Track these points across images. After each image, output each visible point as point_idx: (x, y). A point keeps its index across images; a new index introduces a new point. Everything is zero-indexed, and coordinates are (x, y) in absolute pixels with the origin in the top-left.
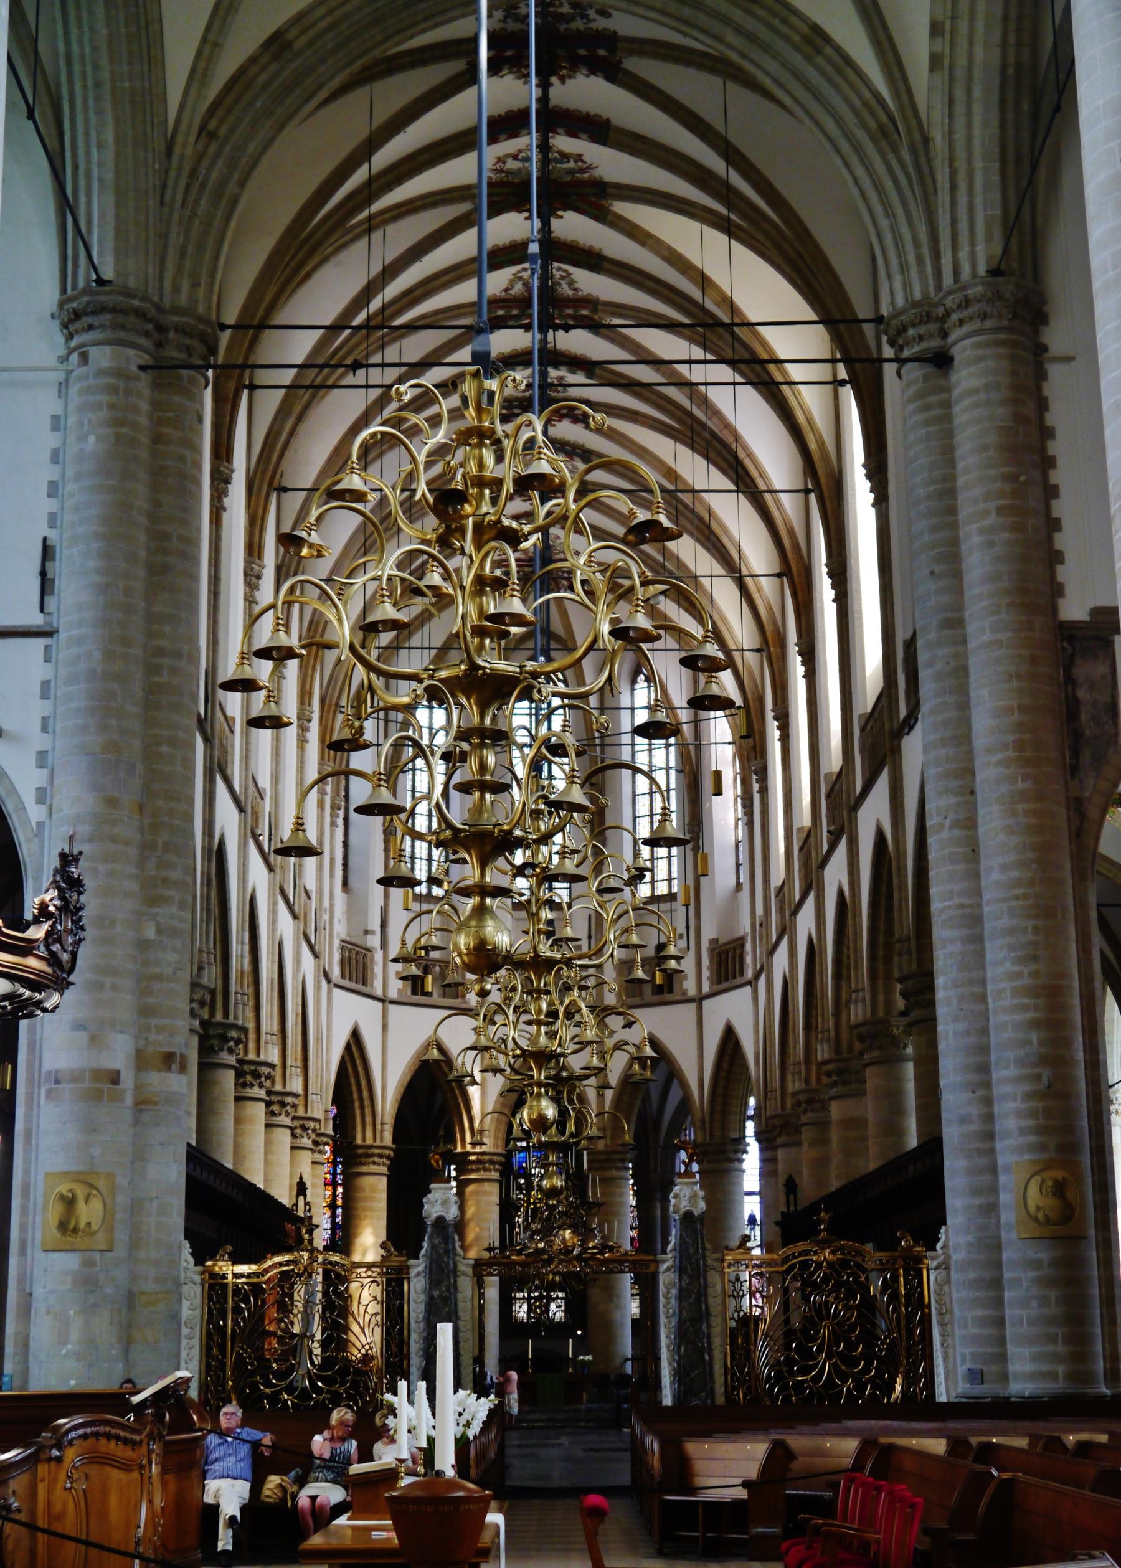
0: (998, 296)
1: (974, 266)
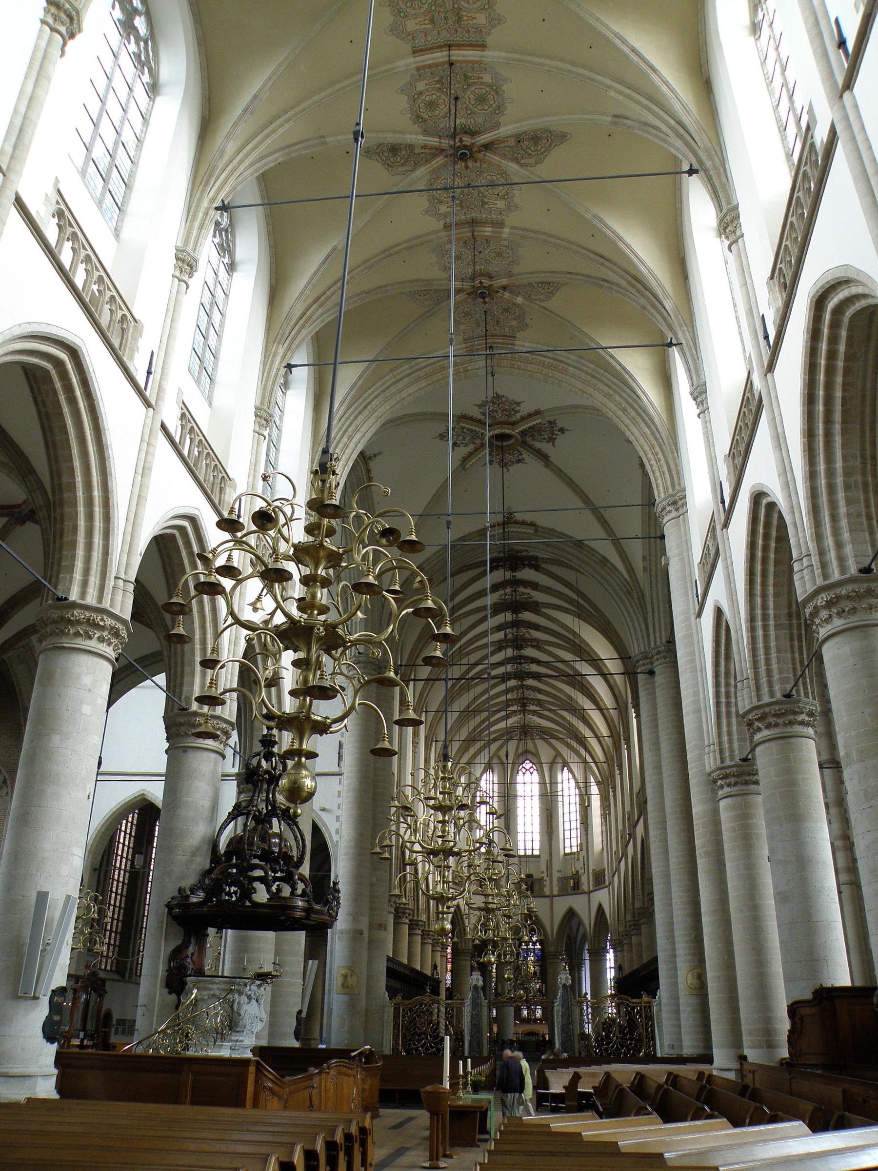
1: (661, 639)
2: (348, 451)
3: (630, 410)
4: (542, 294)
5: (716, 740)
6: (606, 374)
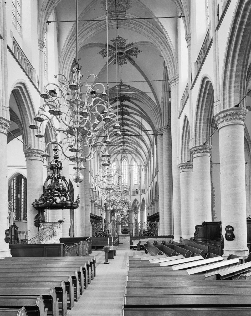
0: (168, 128)
2: (70, 58)
5: (181, 156)
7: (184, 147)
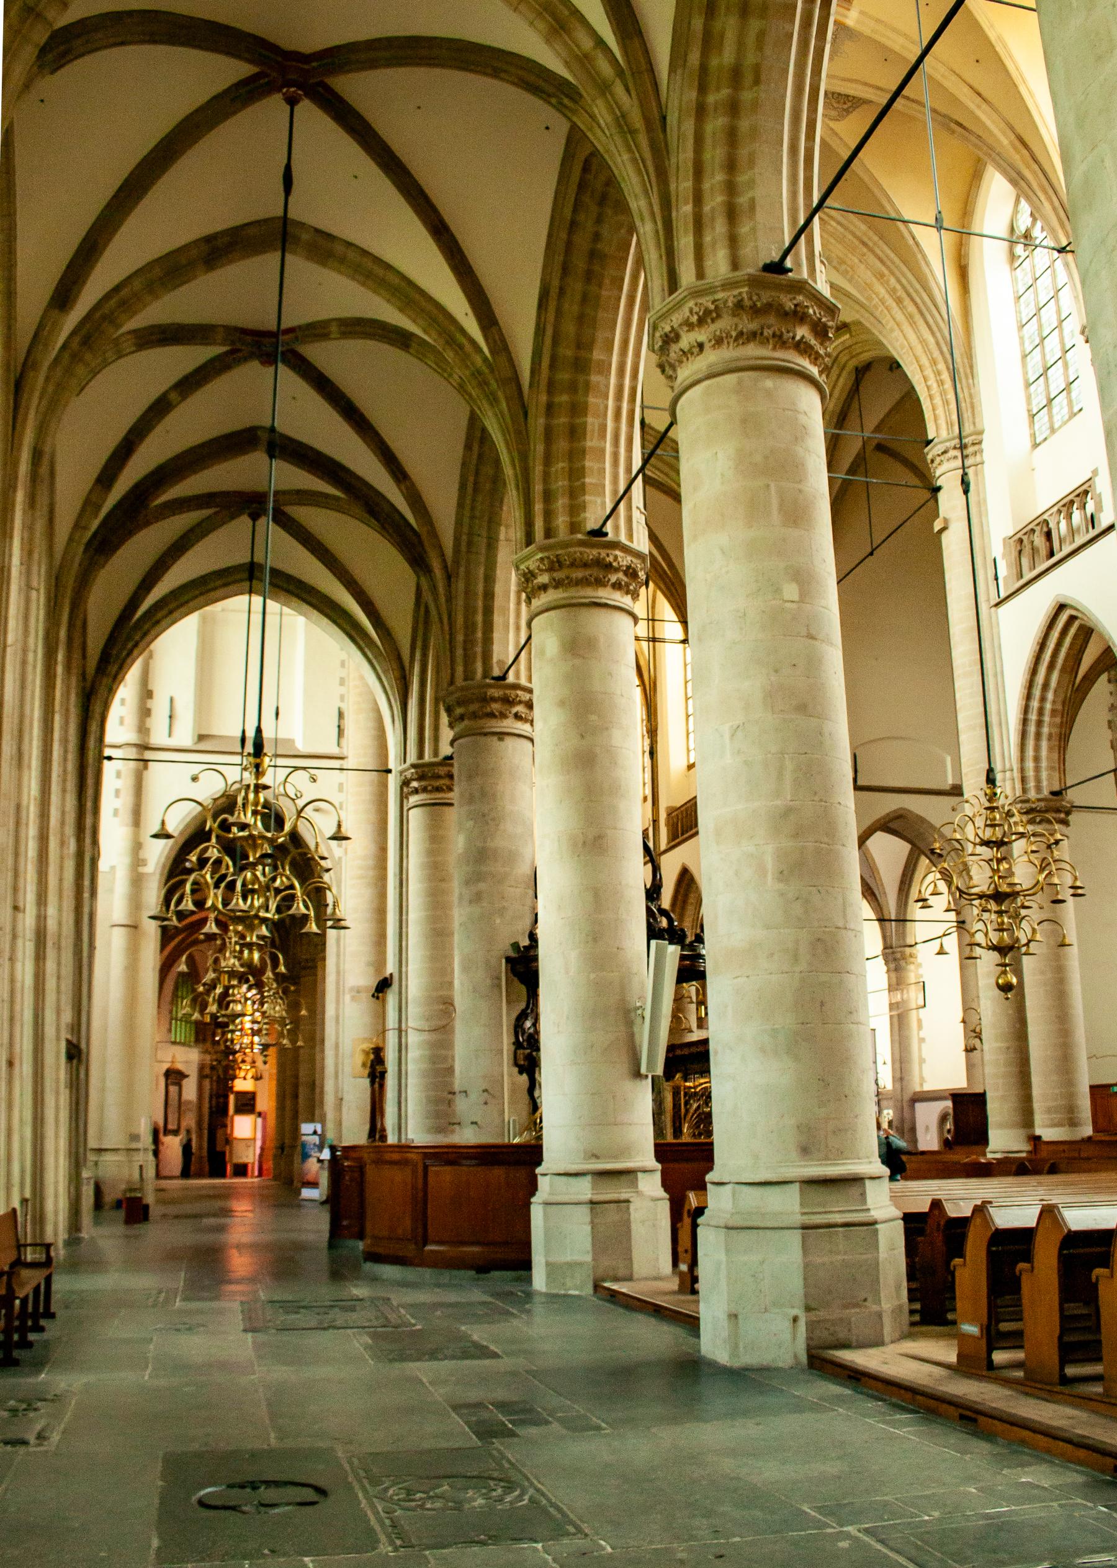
3: (907, 301)
4: (835, 108)
5: (1016, 766)
6: (881, 243)
7: (1032, 729)
